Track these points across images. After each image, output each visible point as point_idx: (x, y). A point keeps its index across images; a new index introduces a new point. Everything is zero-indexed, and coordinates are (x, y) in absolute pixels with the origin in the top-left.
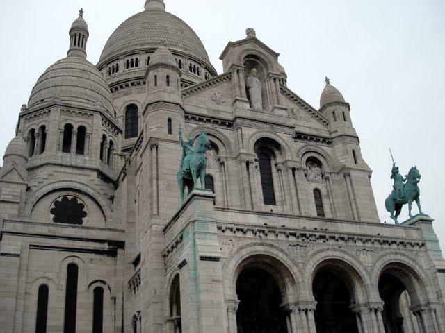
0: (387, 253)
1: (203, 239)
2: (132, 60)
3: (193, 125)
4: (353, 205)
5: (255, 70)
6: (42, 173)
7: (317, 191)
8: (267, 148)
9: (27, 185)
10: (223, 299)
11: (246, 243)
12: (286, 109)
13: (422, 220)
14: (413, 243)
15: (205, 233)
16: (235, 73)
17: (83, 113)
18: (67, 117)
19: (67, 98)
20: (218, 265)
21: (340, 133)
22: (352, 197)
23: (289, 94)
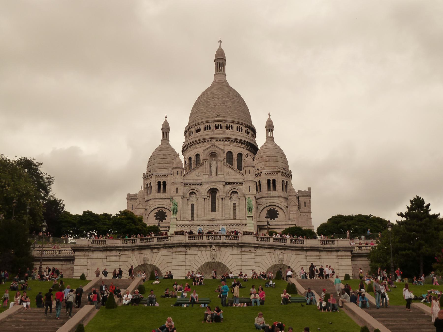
1: (172, 229)
2: (198, 128)
3: (187, 187)
5: (214, 158)
6: (151, 202)
7: (234, 204)
8: (213, 192)
9: (145, 209)
12: (223, 174)
14: (241, 224)
15: (173, 228)
16: (205, 162)
17: (164, 175)
18: (158, 178)
19: (158, 170)
21: (245, 180)
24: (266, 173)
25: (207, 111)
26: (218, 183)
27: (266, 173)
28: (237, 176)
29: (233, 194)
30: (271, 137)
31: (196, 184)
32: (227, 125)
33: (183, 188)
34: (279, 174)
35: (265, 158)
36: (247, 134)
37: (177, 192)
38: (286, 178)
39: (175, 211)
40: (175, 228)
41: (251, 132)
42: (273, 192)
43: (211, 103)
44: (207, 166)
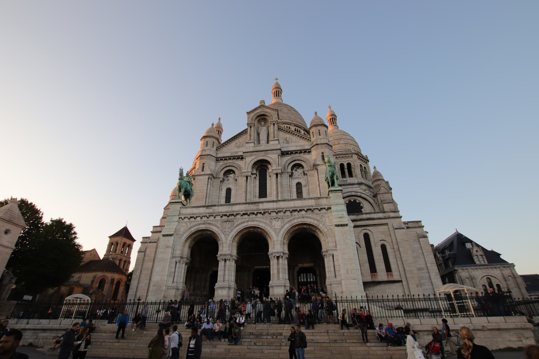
0: (295, 218)
3: (221, 163)
10: (169, 255)
11: (195, 224)
12: (278, 140)
13: (331, 191)
14: (319, 208)
15: (171, 222)
16: (249, 129)
20: (172, 237)
21: (314, 144)
23: (285, 130)
24: (336, 156)
26: (270, 151)
28: (299, 142)
29: (295, 168)
30: (335, 126)
31: (234, 158)
35: (333, 141)
37: (203, 171)
38: (363, 163)
44: (252, 133)
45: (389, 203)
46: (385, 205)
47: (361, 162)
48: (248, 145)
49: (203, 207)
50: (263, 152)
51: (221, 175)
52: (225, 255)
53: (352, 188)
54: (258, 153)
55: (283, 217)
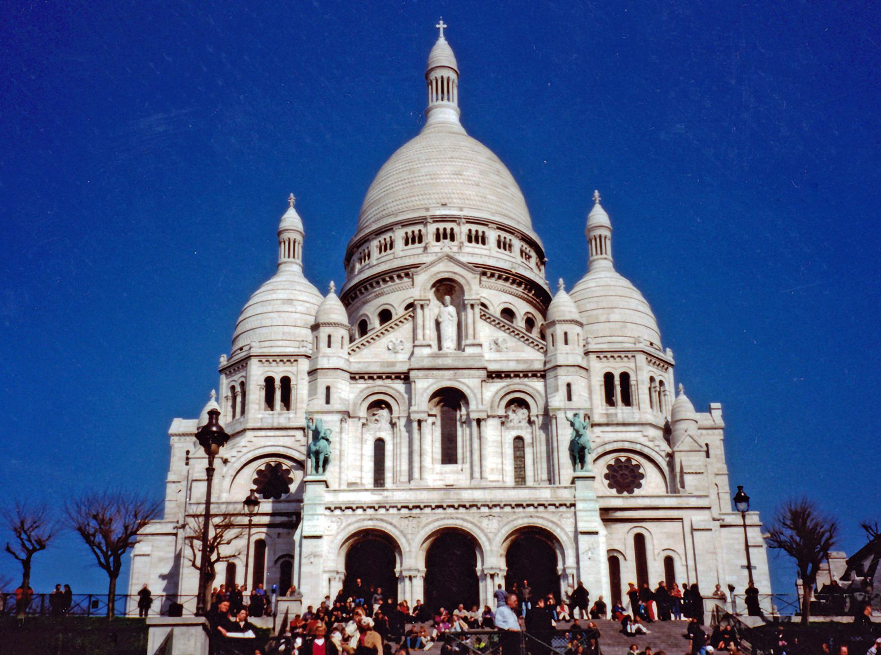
1: (309, 520)
2: (385, 239)
3: (361, 385)
4: (555, 454)
7: (519, 439)
11: (353, 519)
14: (557, 504)
15: (313, 515)
22: (555, 445)
25: (411, 195)
27: (601, 354)
29: (513, 406)
32: (470, 231)
33: (348, 389)
34: (641, 358)
35: (595, 312)
36: (524, 260)
37: (328, 402)
38: (660, 373)
39: (322, 461)
40: (319, 517)
41: (533, 254)
42: (622, 409)
43: (423, 174)
45: (696, 473)
46: (687, 478)
47: (655, 370)
48: (417, 351)
49: (367, 490)
50: (451, 372)
51: (363, 412)
52: (410, 570)
53: (626, 432)
54: (441, 372)
55: (501, 515)
